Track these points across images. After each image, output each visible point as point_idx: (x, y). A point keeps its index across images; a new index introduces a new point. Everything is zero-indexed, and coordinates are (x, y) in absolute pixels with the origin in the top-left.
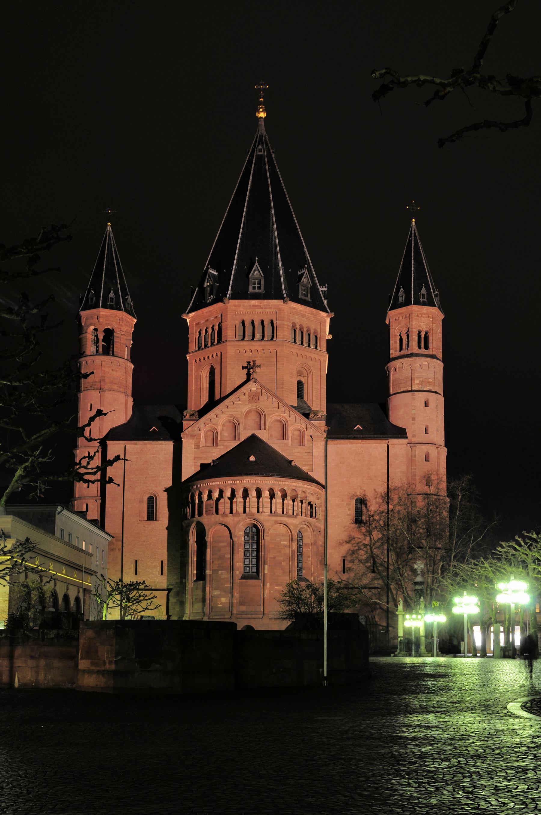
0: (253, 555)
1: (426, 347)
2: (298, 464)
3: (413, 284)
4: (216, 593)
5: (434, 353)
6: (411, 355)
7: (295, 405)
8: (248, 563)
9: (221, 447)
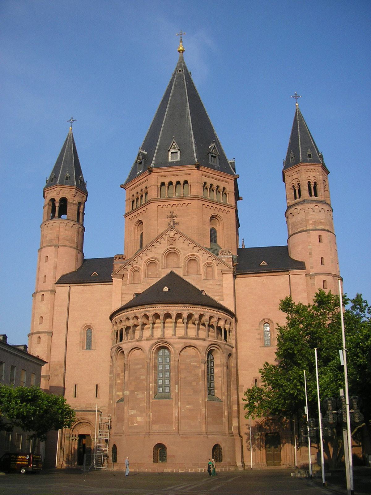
0: (166, 376)
1: (316, 195)
2: (209, 295)
3: (300, 148)
4: (133, 412)
5: (323, 199)
6: (304, 202)
7: (209, 247)
8: (161, 383)
9: (145, 284)
